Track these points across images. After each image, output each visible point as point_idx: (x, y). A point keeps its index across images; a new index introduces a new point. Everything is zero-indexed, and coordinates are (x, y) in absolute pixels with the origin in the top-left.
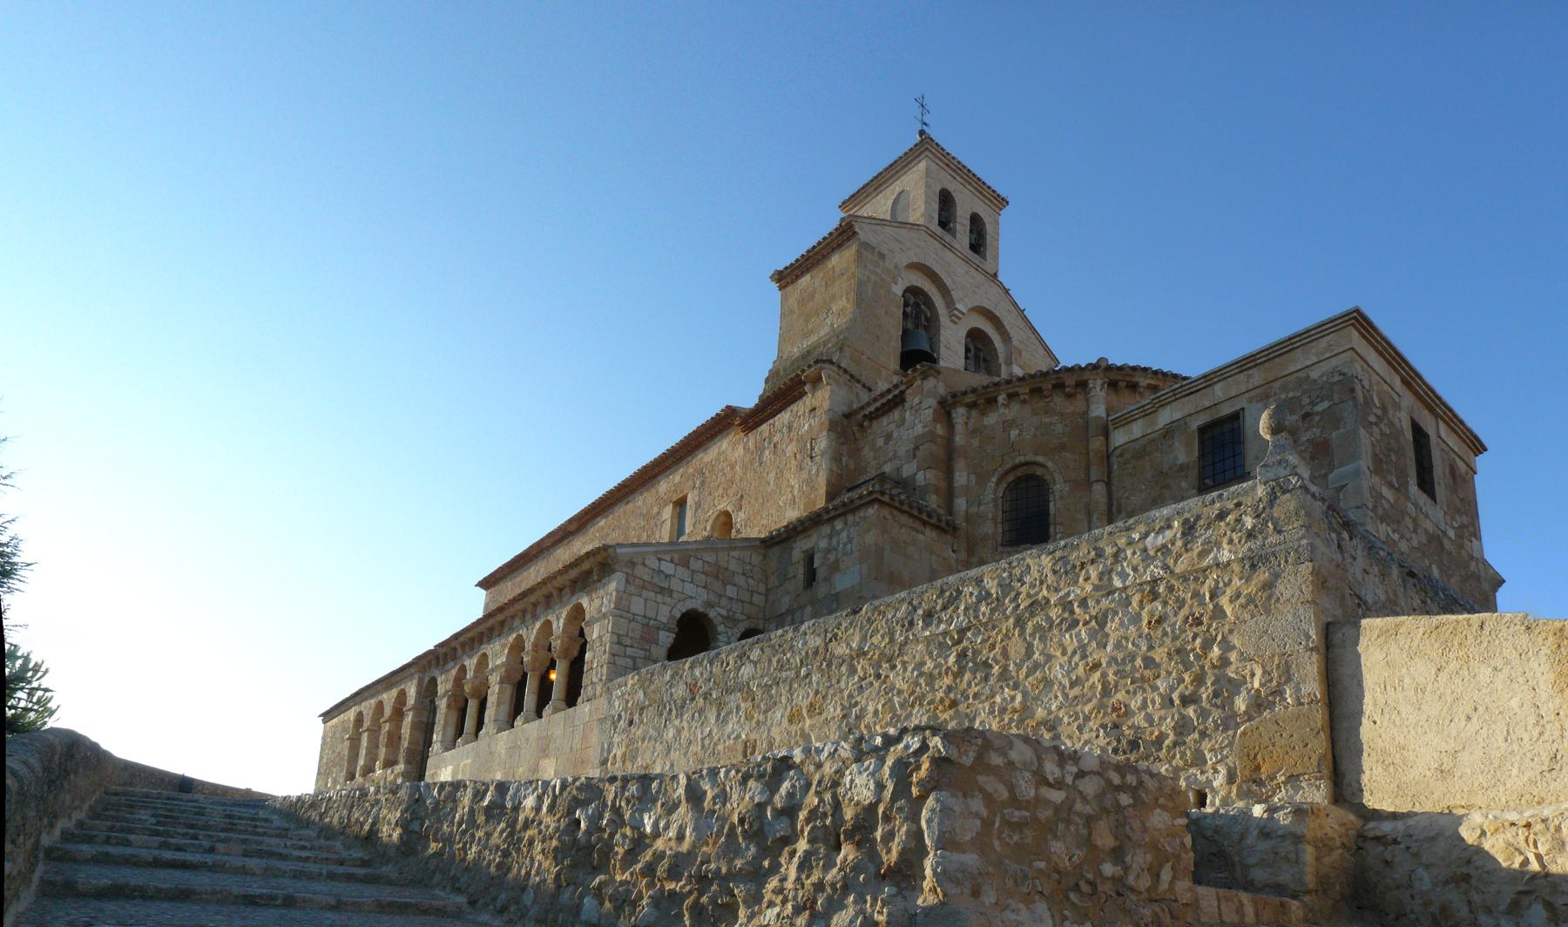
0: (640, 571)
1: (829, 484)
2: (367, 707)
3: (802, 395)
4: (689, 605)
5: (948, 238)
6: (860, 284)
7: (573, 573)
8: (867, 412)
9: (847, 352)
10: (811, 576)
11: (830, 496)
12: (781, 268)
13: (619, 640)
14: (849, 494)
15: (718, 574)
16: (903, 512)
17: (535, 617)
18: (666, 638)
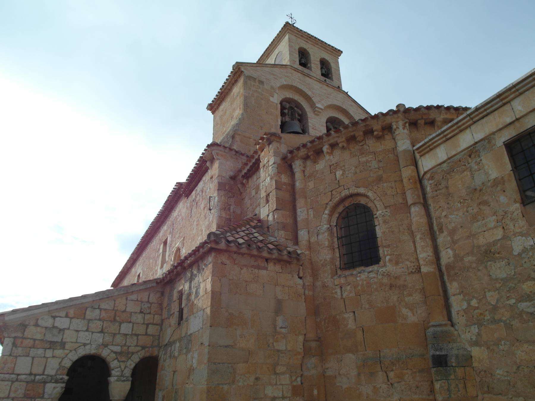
3: (207, 169)
4: (82, 352)
5: (306, 71)
8: (243, 173)
9: (238, 138)
12: (210, 102)
15: (115, 317)
16: (243, 254)
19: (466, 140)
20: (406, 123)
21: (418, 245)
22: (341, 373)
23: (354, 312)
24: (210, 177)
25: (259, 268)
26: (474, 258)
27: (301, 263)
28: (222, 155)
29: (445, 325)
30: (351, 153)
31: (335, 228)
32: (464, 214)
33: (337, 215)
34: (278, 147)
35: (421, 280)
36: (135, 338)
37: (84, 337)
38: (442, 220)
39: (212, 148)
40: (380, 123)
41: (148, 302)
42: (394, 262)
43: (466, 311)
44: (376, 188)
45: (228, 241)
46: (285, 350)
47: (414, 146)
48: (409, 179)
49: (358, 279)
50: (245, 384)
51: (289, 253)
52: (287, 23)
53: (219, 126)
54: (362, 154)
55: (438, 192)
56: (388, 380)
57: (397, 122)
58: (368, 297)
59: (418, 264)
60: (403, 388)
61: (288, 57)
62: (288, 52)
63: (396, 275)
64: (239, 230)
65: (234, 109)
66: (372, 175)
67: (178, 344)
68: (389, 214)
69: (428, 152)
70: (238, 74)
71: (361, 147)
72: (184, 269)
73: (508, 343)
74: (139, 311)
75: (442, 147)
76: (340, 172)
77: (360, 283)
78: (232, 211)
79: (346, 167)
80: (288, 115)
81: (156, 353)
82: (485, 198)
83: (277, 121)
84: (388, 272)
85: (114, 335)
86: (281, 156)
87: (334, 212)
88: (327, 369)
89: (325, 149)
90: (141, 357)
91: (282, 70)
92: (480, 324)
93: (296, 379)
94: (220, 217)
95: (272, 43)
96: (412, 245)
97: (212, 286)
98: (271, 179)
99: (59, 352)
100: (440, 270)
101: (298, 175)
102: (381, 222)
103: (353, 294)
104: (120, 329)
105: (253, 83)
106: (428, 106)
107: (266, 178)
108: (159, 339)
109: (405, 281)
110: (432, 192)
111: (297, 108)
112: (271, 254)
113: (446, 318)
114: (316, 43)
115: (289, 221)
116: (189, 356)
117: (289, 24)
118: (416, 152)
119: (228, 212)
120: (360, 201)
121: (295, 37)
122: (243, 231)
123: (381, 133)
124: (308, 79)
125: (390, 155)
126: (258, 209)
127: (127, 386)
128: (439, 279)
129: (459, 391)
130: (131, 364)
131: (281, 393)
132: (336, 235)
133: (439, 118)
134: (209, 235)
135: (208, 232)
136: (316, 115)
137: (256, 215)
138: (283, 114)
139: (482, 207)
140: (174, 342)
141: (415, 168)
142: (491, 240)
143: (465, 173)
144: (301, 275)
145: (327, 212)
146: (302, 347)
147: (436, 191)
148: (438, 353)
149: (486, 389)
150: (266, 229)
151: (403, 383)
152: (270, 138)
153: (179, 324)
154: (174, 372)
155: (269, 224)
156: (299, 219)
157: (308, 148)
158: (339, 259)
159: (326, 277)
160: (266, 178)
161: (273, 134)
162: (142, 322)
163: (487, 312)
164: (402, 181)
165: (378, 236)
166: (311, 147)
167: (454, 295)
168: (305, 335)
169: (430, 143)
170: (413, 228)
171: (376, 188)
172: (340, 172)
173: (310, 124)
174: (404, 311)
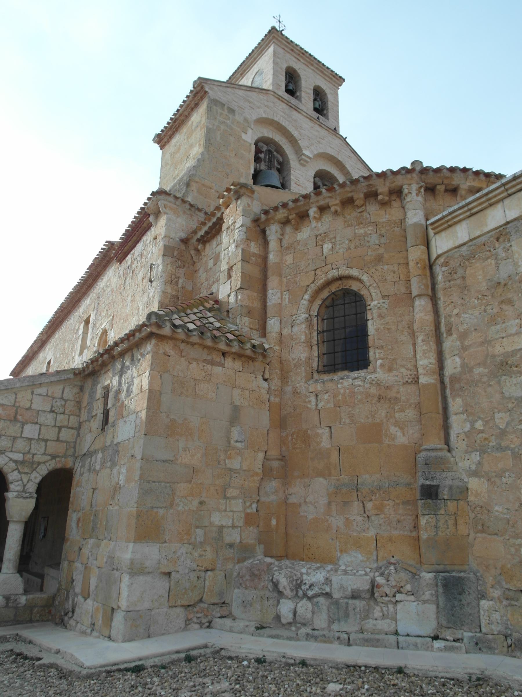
3: (149, 227)
8: (199, 236)
9: (194, 187)
12: (159, 132)
16: (193, 344)
19: (495, 217)
20: (421, 187)
21: (419, 349)
22: (307, 500)
23: (330, 427)
24: (153, 236)
25: (212, 363)
26: (487, 371)
27: (268, 360)
28: (171, 209)
29: (441, 449)
30: (345, 222)
31: (316, 319)
32: (480, 314)
33: (320, 302)
34: (248, 205)
35: (417, 393)
36: (43, 444)
38: (453, 319)
39: (159, 197)
40: (388, 184)
41: (62, 398)
42: (387, 367)
43: (468, 435)
44: (373, 270)
45: (174, 325)
46: (240, 470)
47: (427, 220)
48: (417, 263)
49: (339, 386)
50: (187, 508)
51: (254, 346)
52: (273, 28)
53: (169, 167)
54: (359, 224)
55: (452, 282)
56: (365, 512)
57: (410, 185)
58: (350, 409)
59: (416, 373)
60: (381, 521)
61: (271, 78)
62: (272, 71)
63: (387, 385)
64: (189, 311)
65: (192, 144)
66: (370, 253)
67: (100, 455)
68: (386, 306)
69: (445, 229)
70: (200, 95)
71: (359, 215)
72: (113, 358)
73: (513, 475)
74: (49, 410)
75: (464, 224)
76: (329, 246)
77: (342, 391)
78: (180, 285)
79: (338, 239)
80: (265, 162)
81: (70, 465)
82: (510, 295)
83: (249, 167)
84: (378, 380)
85: (15, 438)
86: (252, 217)
87: (316, 298)
88: (290, 495)
89: (313, 212)
90: (50, 468)
91: (261, 97)
92: (483, 451)
93: (251, 505)
94: (164, 292)
95: (250, 55)
96: (412, 347)
97: (150, 383)
98: (236, 246)
100: (442, 382)
101: (273, 245)
102: (375, 315)
103: (331, 405)
104: (22, 431)
105: (220, 111)
106: (452, 167)
107: (229, 245)
108: (75, 447)
109: (398, 392)
110: (444, 282)
111: (277, 152)
112: (231, 346)
113: (443, 442)
114: (309, 63)
115: (257, 305)
116: (115, 471)
117: (276, 30)
118: (430, 228)
119: (175, 287)
120: (350, 286)
121: (282, 51)
122: (195, 314)
123: (387, 198)
124: (295, 112)
125: (396, 229)
126: (215, 285)
127: (31, 504)
128: (440, 392)
129: (448, 528)
130: (37, 477)
131: (231, 522)
132: (315, 328)
133: (465, 185)
134: (149, 316)
135: (147, 312)
136: (301, 164)
137: (212, 294)
138: (257, 159)
139: (504, 307)
140: (96, 452)
141: (426, 248)
142: (510, 349)
143: (489, 260)
144: (267, 376)
145: (306, 297)
146: (261, 466)
147: (450, 281)
148: (428, 483)
149: (480, 527)
150: (225, 313)
151: (382, 516)
152: (239, 191)
153: (103, 429)
154: (94, 489)
155: (230, 307)
156: (269, 303)
157: (288, 209)
158: (317, 359)
159: (298, 380)
160: (229, 245)
161: (244, 186)
162: (53, 424)
163: (493, 437)
164: (408, 264)
165: (369, 334)
166: (293, 209)
167: (456, 414)
168: (266, 452)
169: (449, 217)
170: (415, 327)
171: (373, 270)
172: (329, 246)
173: (292, 177)
174: (393, 430)
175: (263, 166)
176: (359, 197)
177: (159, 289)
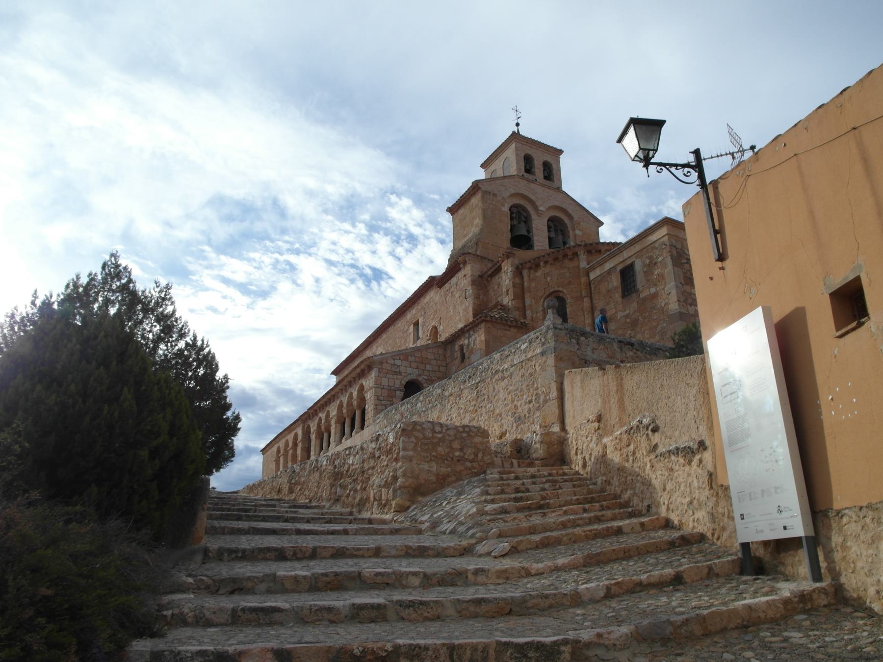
0: (385, 365)
1: (474, 310)
2: (281, 444)
3: (459, 269)
4: (409, 378)
5: (530, 177)
6: (484, 211)
7: (358, 370)
9: (480, 244)
10: (463, 357)
11: (475, 315)
13: (378, 398)
14: (485, 314)
17: (346, 391)
18: (400, 394)
37: (409, 370)
94: (474, 303)
99: (399, 377)
138: (512, 219)
175: (515, 222)
176: (560, 257)
177: (471, 302)
